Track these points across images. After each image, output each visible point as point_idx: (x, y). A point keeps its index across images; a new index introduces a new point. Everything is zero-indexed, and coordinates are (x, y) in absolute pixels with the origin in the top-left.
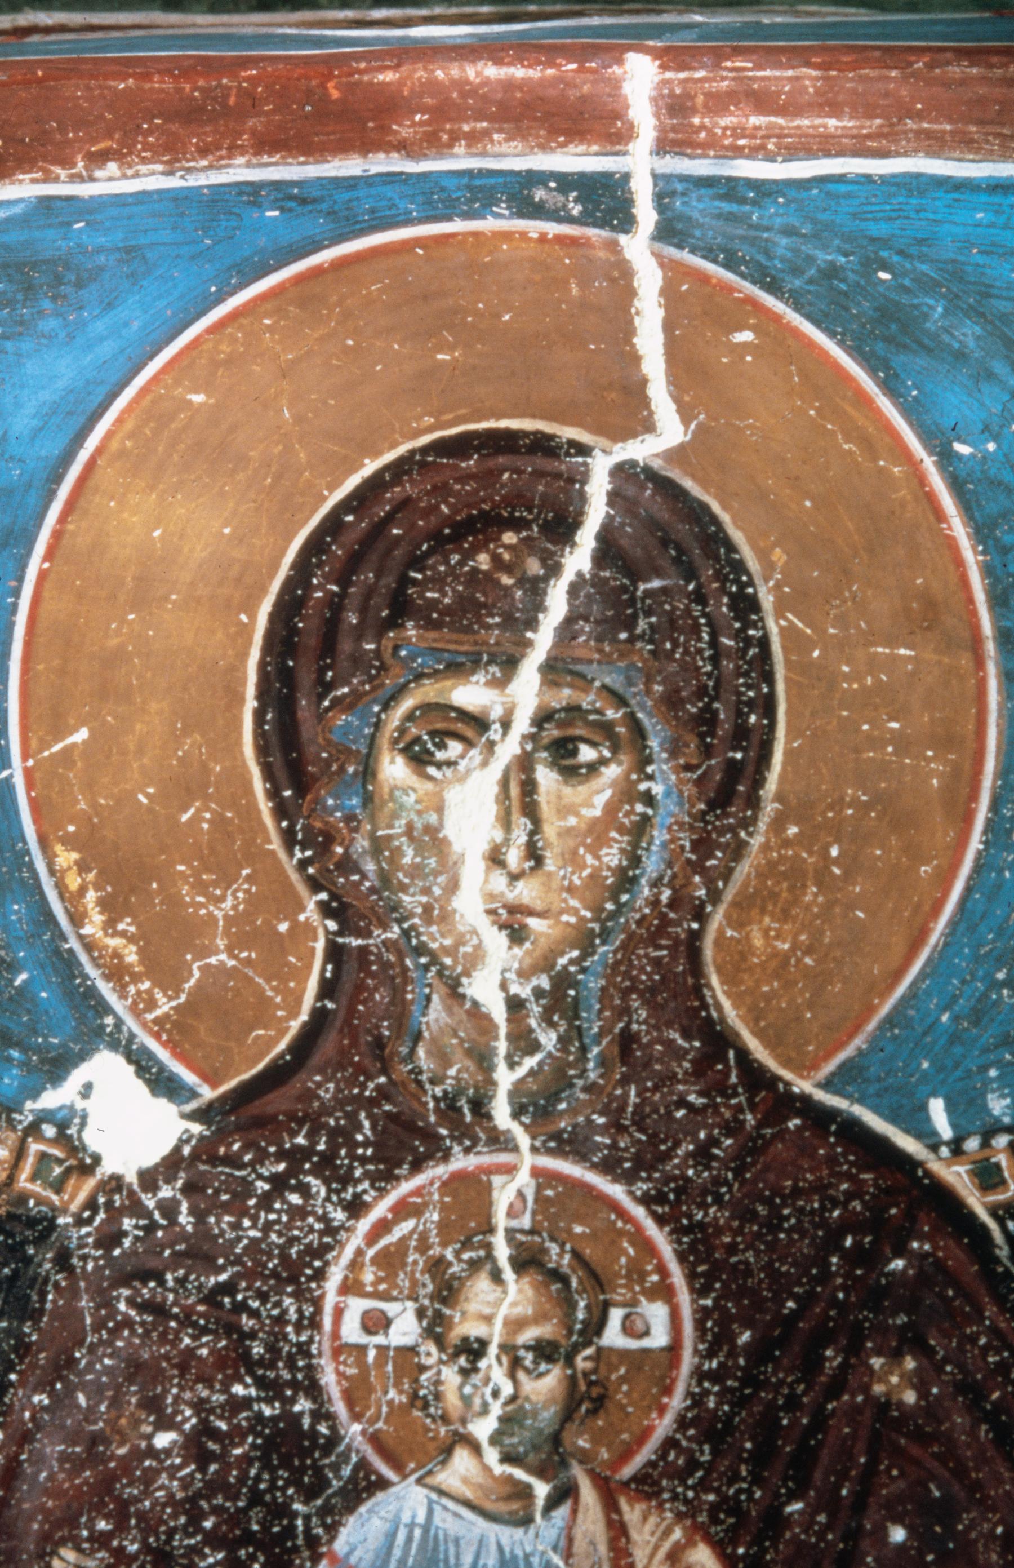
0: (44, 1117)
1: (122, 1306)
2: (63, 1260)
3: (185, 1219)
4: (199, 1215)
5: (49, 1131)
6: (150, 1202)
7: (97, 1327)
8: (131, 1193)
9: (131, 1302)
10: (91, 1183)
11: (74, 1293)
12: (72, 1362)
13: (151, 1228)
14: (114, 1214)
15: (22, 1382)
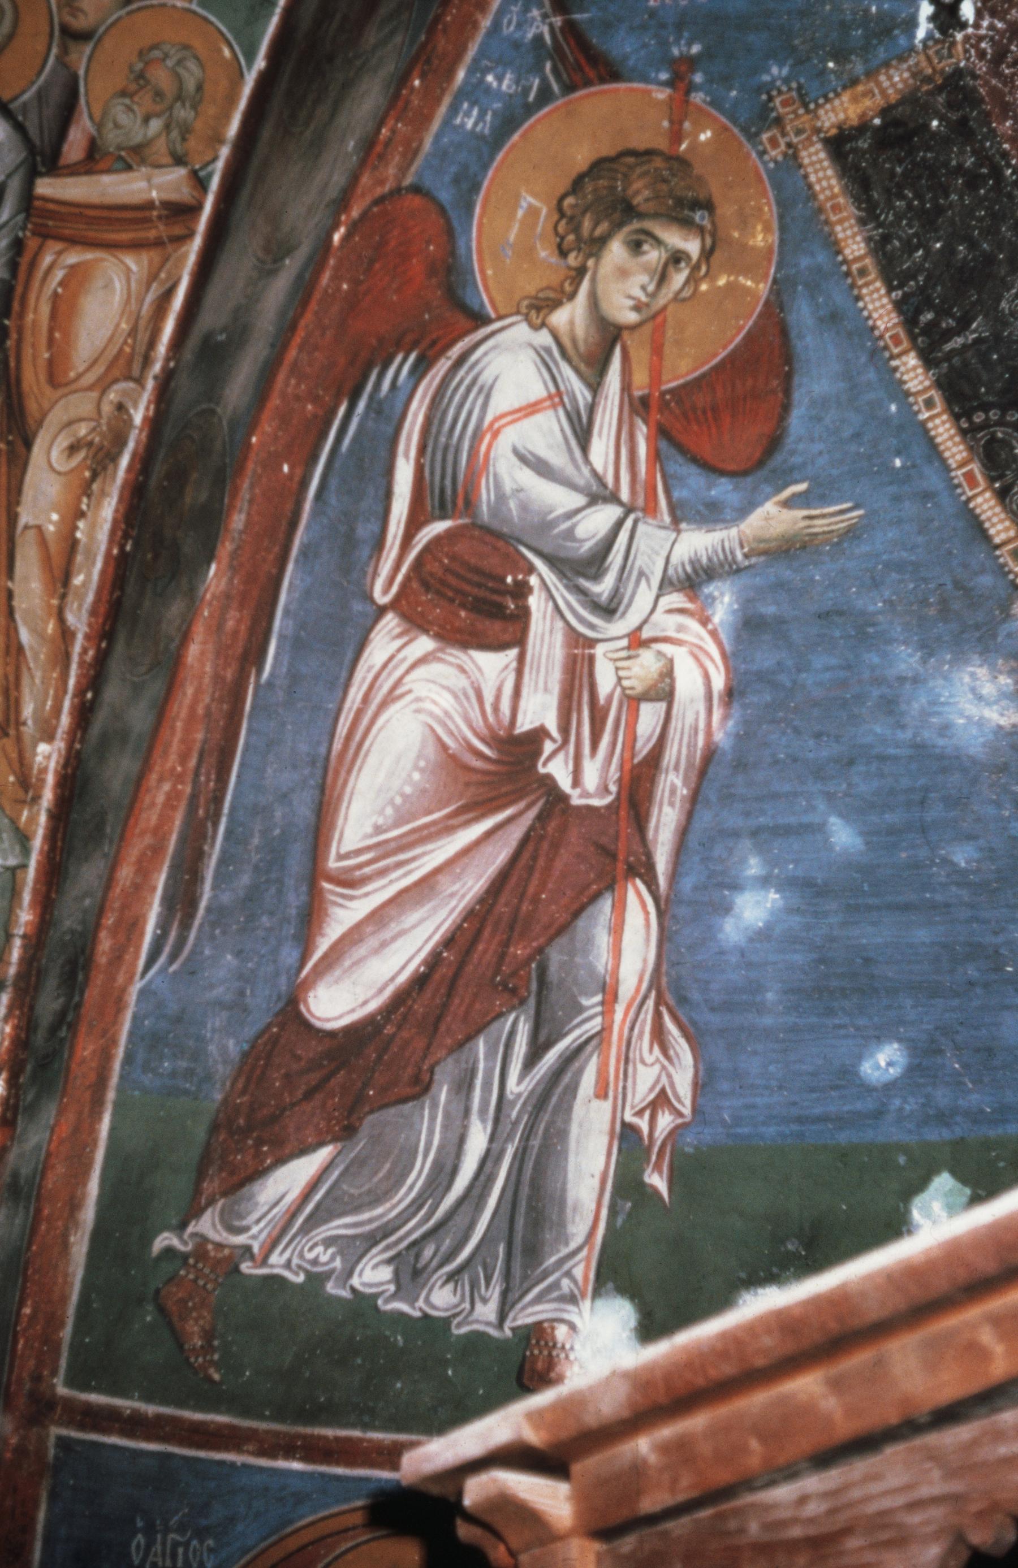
0: (924, 42)
1: (1007, 71)
2: (975, 77)
3: (1000, 25)
4: (1002, 19)
5: (930, 43)
6: (983, 32)
7: (1005, 84)
8: (975, 35)
9: (1008, 67)
10: (960, 48)
11: (987, 83)
12: (1008, 103)
13: (992, 39)
14: (976, 46)
15: (999, 123)
